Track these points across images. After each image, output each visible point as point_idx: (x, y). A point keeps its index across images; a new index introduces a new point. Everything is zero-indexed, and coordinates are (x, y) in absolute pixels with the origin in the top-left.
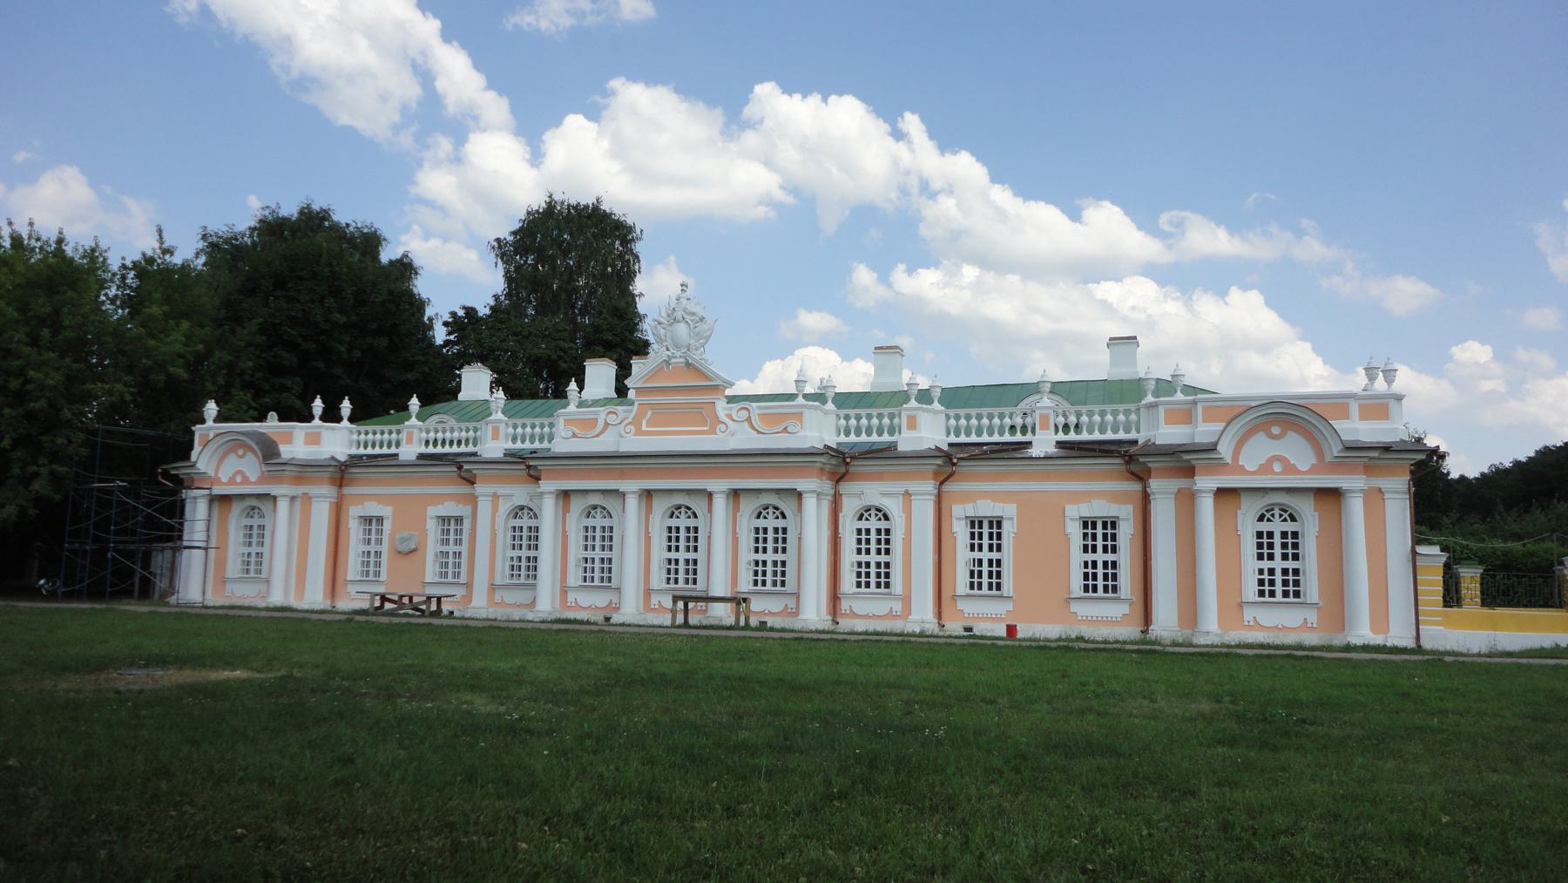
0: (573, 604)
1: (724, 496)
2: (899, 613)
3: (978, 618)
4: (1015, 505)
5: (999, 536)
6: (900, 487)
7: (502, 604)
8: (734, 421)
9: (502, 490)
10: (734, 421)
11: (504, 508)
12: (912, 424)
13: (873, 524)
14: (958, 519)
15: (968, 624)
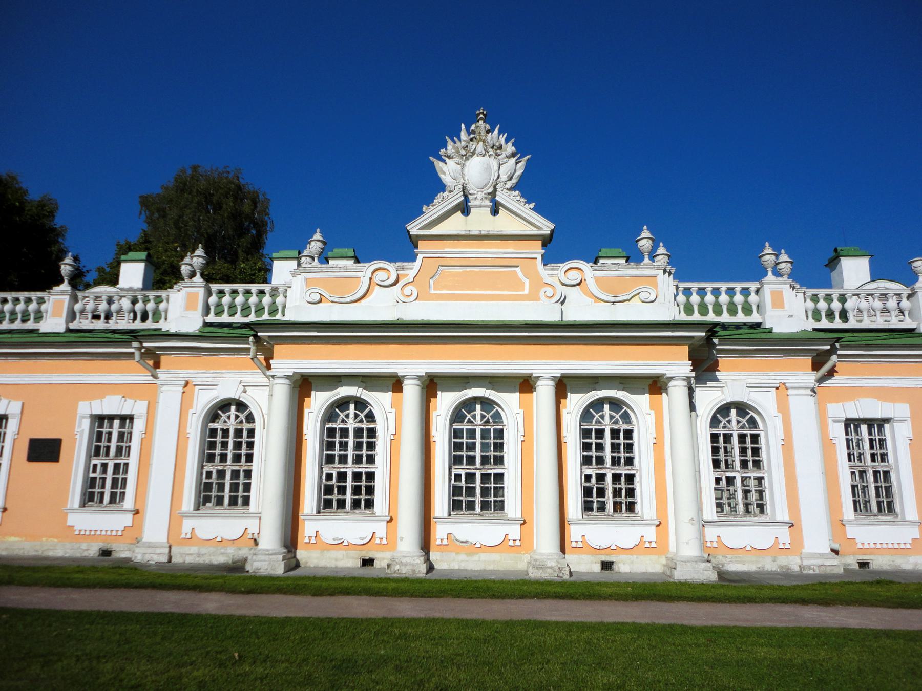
0: (313, 540)
1: (552, 383)
2: (787, 546)
3: (874, 550)
4: (829, 405)
5: (882, 442)
6: (774, 378)
7: (192, 538)
8: (563, 284)
9: (198, 376)
10: (563, 284)
11: (205, 399)
12: (778, 302)
13: (734, 425)
14: (835, 421)
15: (866, 558)
